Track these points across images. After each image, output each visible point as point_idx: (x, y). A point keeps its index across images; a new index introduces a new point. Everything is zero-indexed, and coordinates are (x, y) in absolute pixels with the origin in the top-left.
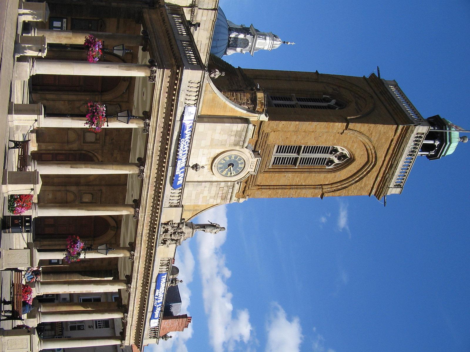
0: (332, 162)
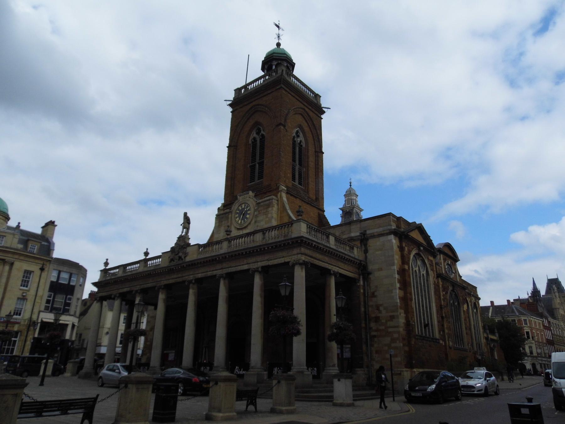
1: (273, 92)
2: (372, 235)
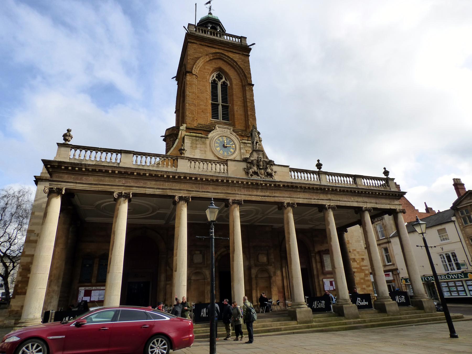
0: (224, 82)
1: (240, 54)
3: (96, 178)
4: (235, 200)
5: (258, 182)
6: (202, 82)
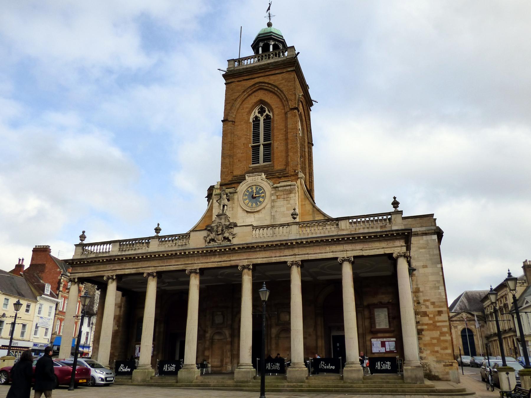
0: (267, 116)
1: (283, 73)
2: (416, 233)
3: (95, 267)
4: (191, 270)
5: (212, 249)
6: (239, 126)
